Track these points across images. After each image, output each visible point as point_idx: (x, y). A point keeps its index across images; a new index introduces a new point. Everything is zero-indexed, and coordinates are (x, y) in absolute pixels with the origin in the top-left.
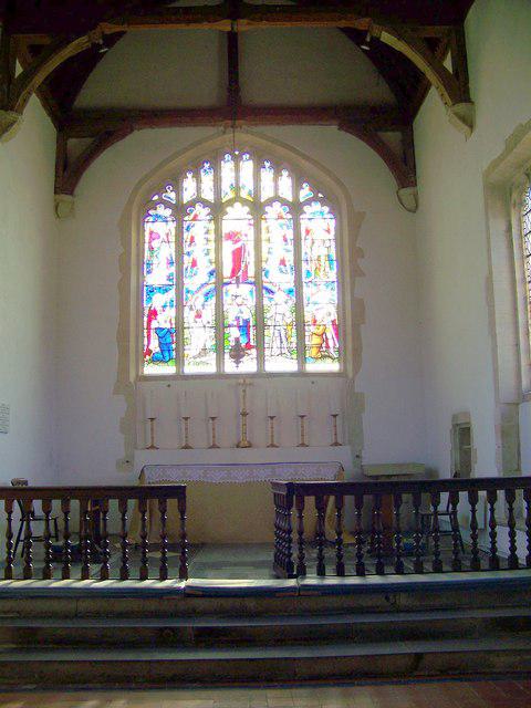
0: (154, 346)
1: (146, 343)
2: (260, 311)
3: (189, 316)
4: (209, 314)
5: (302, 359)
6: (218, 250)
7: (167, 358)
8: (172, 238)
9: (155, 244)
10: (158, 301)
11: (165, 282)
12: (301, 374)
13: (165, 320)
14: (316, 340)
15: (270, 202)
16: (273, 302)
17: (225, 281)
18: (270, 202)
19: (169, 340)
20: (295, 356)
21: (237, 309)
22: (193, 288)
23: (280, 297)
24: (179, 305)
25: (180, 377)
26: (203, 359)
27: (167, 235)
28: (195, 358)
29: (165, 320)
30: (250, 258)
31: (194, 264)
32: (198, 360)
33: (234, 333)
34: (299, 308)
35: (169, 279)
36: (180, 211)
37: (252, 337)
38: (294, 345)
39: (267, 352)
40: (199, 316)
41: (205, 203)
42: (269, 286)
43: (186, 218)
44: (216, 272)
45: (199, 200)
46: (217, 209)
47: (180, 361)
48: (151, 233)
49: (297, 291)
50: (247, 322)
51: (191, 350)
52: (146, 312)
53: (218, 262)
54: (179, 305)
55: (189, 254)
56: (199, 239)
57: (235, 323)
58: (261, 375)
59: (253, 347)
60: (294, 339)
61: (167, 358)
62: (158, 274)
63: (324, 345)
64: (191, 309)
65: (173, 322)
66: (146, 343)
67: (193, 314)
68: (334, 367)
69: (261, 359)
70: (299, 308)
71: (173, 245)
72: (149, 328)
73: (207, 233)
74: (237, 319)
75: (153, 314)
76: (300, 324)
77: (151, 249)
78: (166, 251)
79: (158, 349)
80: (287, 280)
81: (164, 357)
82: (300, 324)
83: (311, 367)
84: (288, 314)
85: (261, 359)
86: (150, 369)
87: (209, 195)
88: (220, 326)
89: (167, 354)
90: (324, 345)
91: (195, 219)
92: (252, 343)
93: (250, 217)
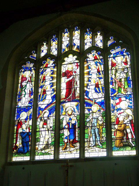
0: (19, 143)
1: (15, 142)
2: (82, 118)
3: (40, 124)
4: (51, 123)
5: (110, 149)
6: (59, 82)
7: (26, 151)
8: (33, 79)
9: (24, 84)
10: (24, 115)
11: (27, 104)
12: (109, 158)
13: (25, 128)
14: (119, 135)
15: (90, 50)
16: (91, 111)
17: (62, 100)
18: (90, 50)
19: (28, 139)
20: (104, 146)
21: (68, 118)
22: (43, 107)
23: (95, 108)
24: (34, 117)
25: (33, 162)
26: (47, 151)
27: (31, 78)
28: (41, 150)
29: (25, 128)
30: (77, 86)
31: (45, 92)
32: (43, 151)
33: (66, 133)
34: (107, 115)
35: (30, 103)
36: (39, 64)
37: (77, 135)
38: (104, 139)
39: (86, 144)
40: (45, 123)
41: (52, 57)
42: (89, 101)
43: (42, 67)
44: (57, 97)
45: (49, 56)
46: (59, 60)
47: (33, 153)
48: (23, 77)
49: (106, 105)
50: (74, 125)
51: (40, 146)
52: (16, 123)
53: (58, 90)
54: (34, 117)
55: (42, 87)
56: (48, 77)
57: (67, 127)
58: (82, 159)
59: (77, 141)
60: (104, 135)
61: (26, 151)
62: (24, 101)
63: (125, 138)
64: (41, 120)
65: (31, 128)
66: (15, 142)
67: (42, 123)
68: (134, 153)
69: (82, 150)
70: (107, 115)
71: (33, 83)
72: (17, 133)
73: (52, 74)
74: (68, 124)
75: (20, 124)
76: (108, 124)
77: (22, 86)
78: (29, 87)
79: (21, 145)
80: (100, 97)
81: (24, 150)
82: (108, 124)
83: (116, 153)
84: (100, 118)
85: (82, 150)
86: (16, 159)
87: (55, 52)
88: (58, 128)
89: (26, 148)
90: (125, 138)
91: (46, 67)
92: (77, 139)
93: (77, 61)
